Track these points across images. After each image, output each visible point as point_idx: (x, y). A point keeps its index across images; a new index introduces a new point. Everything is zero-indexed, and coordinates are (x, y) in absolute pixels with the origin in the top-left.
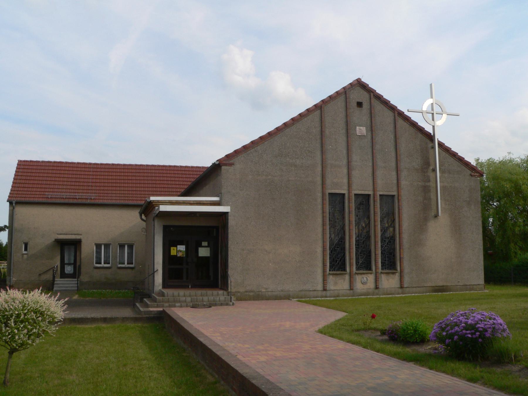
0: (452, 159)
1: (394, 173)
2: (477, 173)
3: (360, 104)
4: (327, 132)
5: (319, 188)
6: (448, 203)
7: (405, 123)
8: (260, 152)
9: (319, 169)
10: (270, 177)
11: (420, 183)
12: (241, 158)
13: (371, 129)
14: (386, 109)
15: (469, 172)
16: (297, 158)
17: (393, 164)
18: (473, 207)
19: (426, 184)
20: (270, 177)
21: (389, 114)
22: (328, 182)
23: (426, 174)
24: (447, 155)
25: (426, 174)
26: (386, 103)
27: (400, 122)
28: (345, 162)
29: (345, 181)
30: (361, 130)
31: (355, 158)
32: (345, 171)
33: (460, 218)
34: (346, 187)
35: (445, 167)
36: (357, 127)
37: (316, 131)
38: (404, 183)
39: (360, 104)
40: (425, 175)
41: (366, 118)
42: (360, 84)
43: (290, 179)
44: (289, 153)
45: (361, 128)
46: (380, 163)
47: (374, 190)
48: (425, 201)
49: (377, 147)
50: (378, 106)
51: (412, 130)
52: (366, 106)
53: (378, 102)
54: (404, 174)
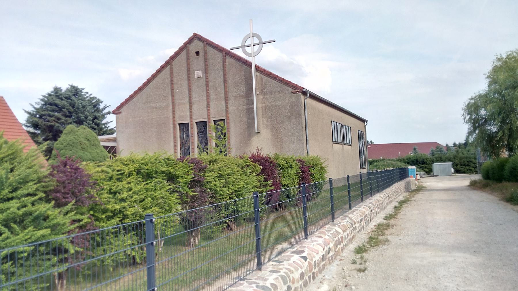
0: (274, 81)
1: (223, 102)
2: (298, 89)
3: (197, 53)
4: (175, 80)
5: (171, 121)
6: (269, 120)
7: (233, 60)
8: (135, 102)
9: (171, 108)
10: (142, 118)
11: (245, 107)
12: (125, 108)
13: (206, 71)
14: (217, 52)
15: (291, 90)
16: (157, 102)
17: (223, 95)
18: (293, 120)
19: (250, 106)
20: (142, 118)
21: (220, 55)
22: (177, 116)
23: (249, 99)
24: (269, 79)
25: (249, 99)
26: (217, 48)
27: (229, 60)
28: (187, 100)
29: (188, 113)
30: (199, 73)
31: (194, 95)
32: (188, 106)
33: (281, 131)
34: (189, 118)
35: (267, 89)
36: (195, 72)
37: (168, 81)
38: (231, 108)
39: (197, 53)
40: (249, 100)
41: (202, 63)
42: (196, 37)
43: (153, 117)
44: (152, 100)
45: (198, 71)
46: (212, 96)
47: (209, 117)
48: (249, 121)
49: (210, 84)
50: (211, 51)
51: (238, 64)
52: (201, 54)
53: (210, 48)
54: (230, 102)
